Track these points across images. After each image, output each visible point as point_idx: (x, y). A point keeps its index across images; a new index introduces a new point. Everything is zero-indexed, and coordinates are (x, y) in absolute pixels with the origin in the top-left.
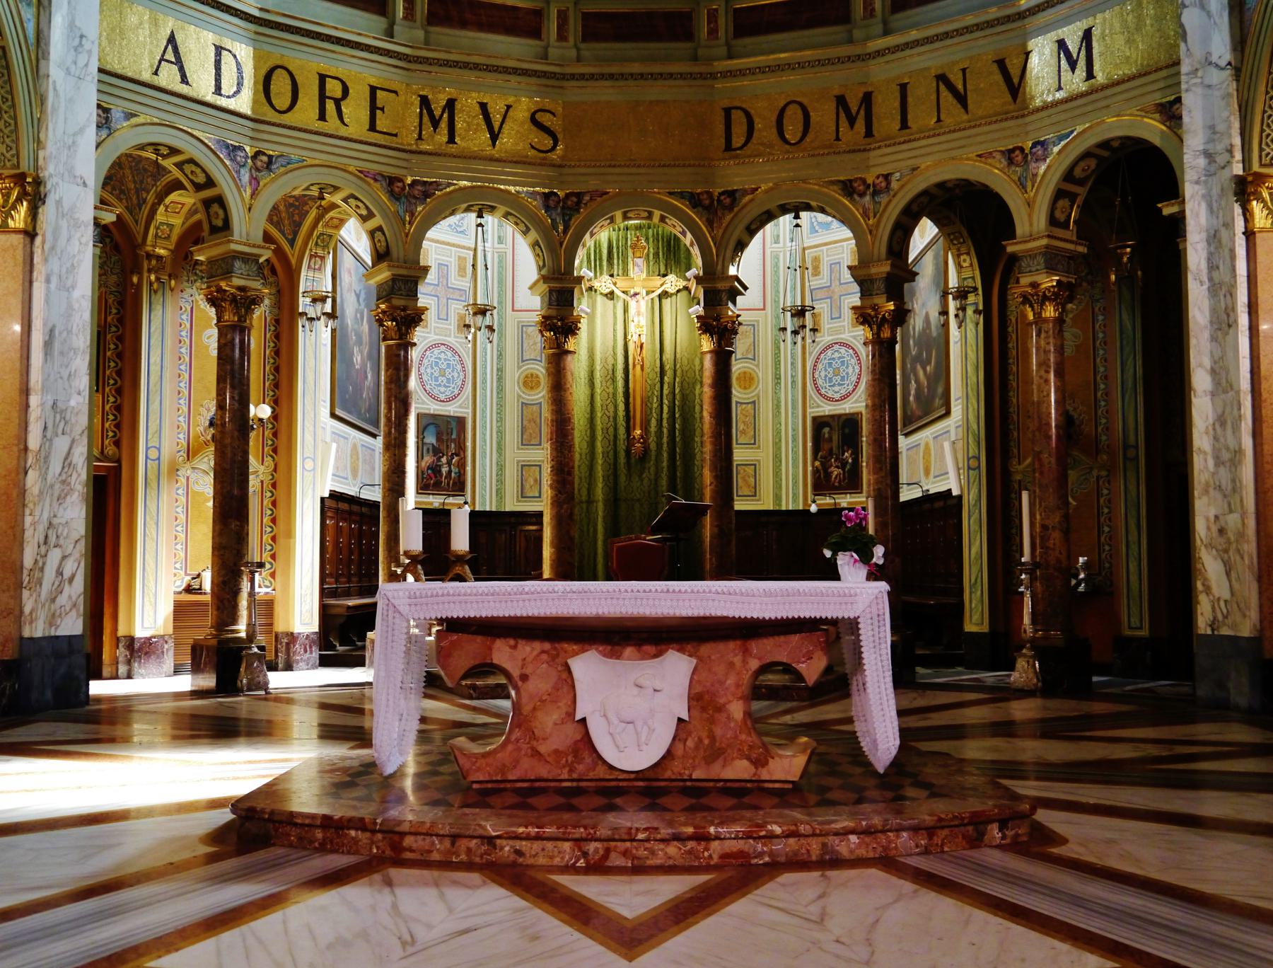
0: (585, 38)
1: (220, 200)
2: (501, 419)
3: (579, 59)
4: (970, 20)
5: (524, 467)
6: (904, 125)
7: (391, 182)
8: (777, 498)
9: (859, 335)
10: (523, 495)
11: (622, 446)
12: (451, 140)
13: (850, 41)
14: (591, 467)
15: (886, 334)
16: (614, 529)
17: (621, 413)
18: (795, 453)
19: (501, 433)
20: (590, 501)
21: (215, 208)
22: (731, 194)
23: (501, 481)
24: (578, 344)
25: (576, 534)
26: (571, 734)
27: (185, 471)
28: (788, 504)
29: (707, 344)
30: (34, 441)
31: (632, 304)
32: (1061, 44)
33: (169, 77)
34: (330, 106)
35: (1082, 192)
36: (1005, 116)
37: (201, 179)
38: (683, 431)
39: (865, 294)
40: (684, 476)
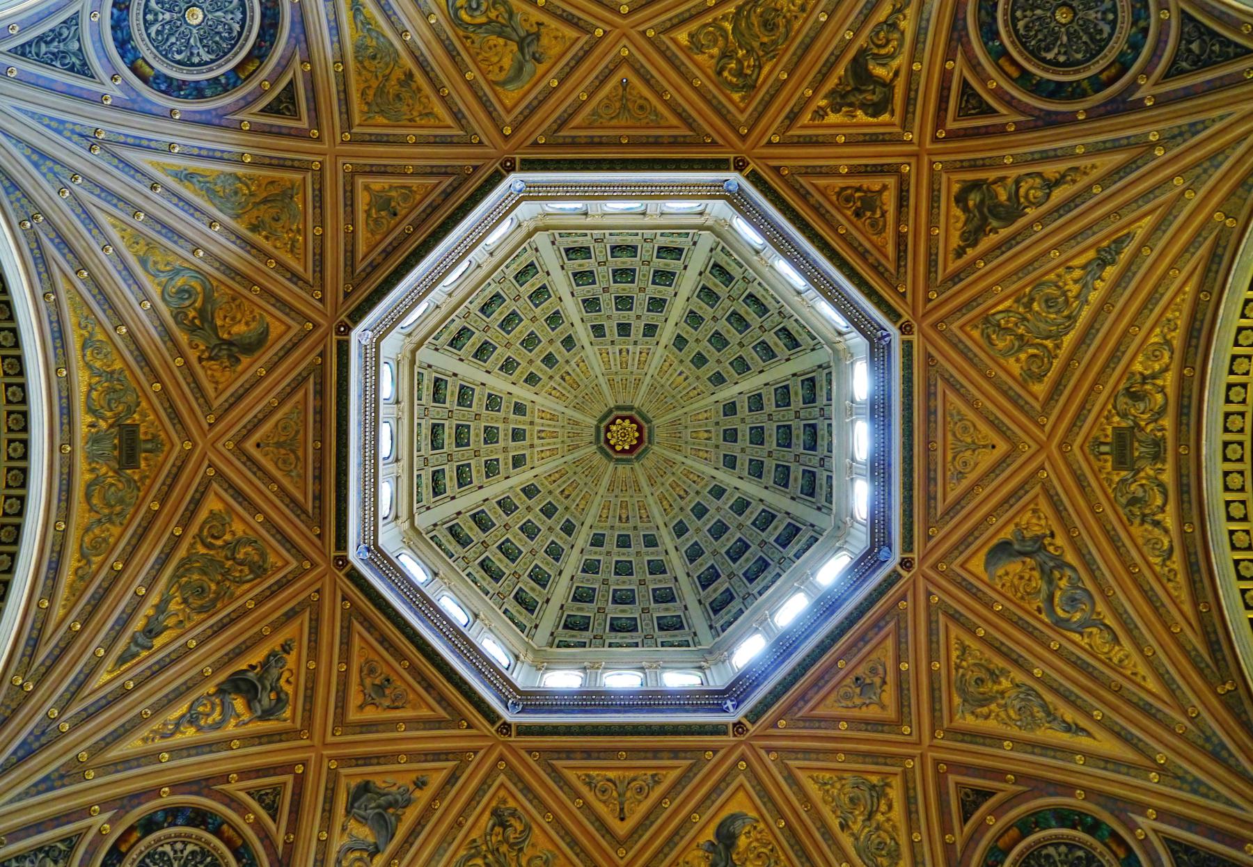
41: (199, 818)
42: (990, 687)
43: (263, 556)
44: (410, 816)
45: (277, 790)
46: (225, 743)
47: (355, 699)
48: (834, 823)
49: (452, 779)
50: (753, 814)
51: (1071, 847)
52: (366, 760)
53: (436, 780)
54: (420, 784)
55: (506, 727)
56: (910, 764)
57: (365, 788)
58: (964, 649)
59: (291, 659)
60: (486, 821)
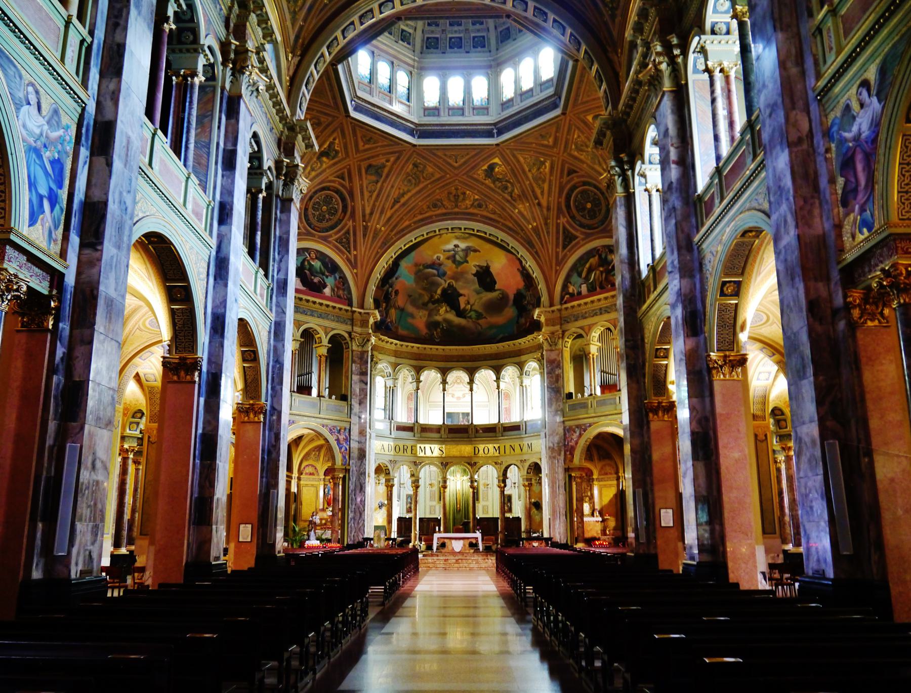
5: (431, 507)
9: (498, 489)
10: (431, 513)
16: (454, 525)
19: (425, 498)
23: (425, 509)
24: (447, 490)
29: (471, 490)
33: (382, 452)
36: (520, 454)
40: (467, 517)
41: (323, 189)
42: (584, 148)
43: (319, 120)
44: (386, 170)
45: (343, 174)
46: (324, 170)
47: (361, 144)
48: (527, 169)
49: (398, 158)
50: (500, 163)
51: (595, 194)
52: (368, 158)
53: (392, 159)
54: (388, 161)
55: (415, 146)
56: (554, 158)
57: (370, 166)
58: (579, 137)
59: (337, 141)
60: (411, 166)
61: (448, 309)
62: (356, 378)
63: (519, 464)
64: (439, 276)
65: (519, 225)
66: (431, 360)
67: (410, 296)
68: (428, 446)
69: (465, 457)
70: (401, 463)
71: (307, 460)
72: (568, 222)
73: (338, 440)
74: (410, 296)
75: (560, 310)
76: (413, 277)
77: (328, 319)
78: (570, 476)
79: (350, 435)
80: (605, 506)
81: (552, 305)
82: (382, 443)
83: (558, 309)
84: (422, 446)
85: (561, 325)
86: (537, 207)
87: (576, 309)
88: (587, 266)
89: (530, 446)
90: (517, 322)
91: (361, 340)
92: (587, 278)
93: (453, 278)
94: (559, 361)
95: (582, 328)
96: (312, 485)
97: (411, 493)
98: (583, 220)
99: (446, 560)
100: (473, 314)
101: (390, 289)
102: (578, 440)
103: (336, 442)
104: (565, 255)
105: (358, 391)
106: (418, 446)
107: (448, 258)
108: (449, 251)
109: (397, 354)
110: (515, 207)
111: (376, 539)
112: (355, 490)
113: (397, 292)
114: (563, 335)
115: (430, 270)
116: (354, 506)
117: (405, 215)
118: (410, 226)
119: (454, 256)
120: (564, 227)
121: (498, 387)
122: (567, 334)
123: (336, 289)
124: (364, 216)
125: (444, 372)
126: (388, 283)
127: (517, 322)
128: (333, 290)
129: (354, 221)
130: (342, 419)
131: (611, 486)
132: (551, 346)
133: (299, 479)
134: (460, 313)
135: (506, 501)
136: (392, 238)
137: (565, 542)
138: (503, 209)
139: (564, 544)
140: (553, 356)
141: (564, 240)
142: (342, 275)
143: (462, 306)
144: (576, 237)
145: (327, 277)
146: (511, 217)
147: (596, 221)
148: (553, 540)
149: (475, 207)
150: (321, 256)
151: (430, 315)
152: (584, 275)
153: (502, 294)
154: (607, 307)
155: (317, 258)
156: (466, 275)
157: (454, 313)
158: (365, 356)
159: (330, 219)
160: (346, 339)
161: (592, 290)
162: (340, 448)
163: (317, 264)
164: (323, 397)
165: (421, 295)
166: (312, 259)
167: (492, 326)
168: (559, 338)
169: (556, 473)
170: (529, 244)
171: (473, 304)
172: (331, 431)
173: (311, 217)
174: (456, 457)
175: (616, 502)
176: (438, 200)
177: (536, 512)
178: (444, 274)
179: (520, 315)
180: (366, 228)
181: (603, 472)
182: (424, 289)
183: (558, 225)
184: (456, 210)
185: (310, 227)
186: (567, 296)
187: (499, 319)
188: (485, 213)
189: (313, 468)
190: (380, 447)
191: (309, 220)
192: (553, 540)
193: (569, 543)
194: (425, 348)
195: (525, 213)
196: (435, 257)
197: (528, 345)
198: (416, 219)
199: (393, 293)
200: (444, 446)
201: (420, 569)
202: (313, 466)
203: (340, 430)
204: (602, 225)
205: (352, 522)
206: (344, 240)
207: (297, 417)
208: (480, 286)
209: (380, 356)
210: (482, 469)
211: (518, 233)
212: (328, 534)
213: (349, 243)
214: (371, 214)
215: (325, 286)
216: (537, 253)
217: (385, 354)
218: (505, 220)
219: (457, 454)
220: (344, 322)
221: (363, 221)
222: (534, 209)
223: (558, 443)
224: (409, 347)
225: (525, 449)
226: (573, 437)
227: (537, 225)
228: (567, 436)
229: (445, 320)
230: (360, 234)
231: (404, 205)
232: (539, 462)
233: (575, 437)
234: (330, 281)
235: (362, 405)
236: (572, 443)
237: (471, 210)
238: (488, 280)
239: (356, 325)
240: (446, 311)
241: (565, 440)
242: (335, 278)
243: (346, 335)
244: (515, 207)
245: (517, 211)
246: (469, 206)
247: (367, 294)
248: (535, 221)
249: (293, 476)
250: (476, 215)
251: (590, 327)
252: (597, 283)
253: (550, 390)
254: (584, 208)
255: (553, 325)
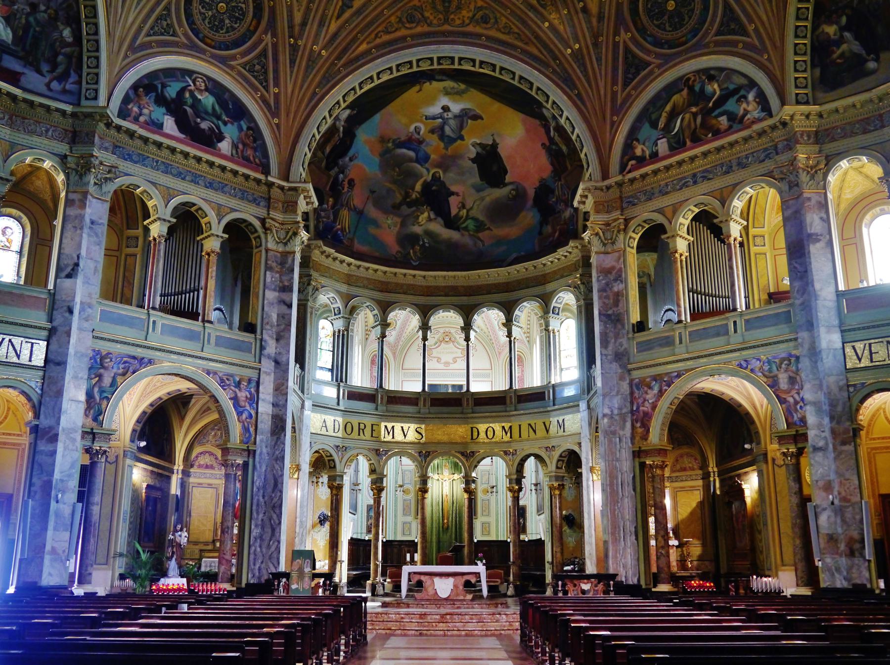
0: (431, 406)
1: (333, 460)
2: (396, 506)
3: (429, 413)
4: (536, 410)
6: (520, 436)
7: (377, 450)
8: (497, 535)
9: (510, 494)
10: (404, 534)
11: (441, 525)
12: (393, 438)
13: (506, 411)
14: (432, 532)
15: (516, 495)
16: (439, 551)
17: (441, 515)
18: (503, 519)
19: (396, 511)
20: (431, 542)
21: (331, 462)
22: (473, 452)
23: (396, 529)
24: (428, 496)
25: (427, 552)
26: (434, 591)
27: (312, 532)
28: (501, 538)
29: (466, 496)
30: (297, 530)
31: (444, 483)
32: (558, 421)
33: (324, 432)
34: (361, 431)
35: (566, 459)
36: (545, 438)
37: (329, 455)
38: (459, 521)
39: (510, 483)
40: (459, 537)
61: (432, 216)
62: (271, 295)
63: (543, 454)
64: (417, 161)
65: (550, 51)
66: (405, 293)
67: (373, 192)
68: (398, 426)
69: (456, 443)
70: (355, 452)
71: (202, 444)
72: (633, 39)
73: (235, 399)
74: (373, 192)
75: (620, 185)
76: (377, 160)
77: (224, 192)
78: (643, 465)
79: (258, 391)
80: (683, 521)
81: (605, 176)
82: (324, 417)
83: (616, 183)
84: (389, 425)
85: (622, 210)
86: (581, 15)
87: (648, 180)
88: (668, 108)
89: (562, 425)
90: (540, 233)
91: (282, 234)
92: (668, 128)
93: (439, 165)
94: (621, 268)
95: (660, 211)
96: (210, 486)
97: (372, 502)
98: (660, 34)
99: (422, 616)
100: (470, 224)
101: (341, 176)
102: (658, 400)
103: (231, 403)
104: (629, 95)
105: (274, 317)
106: (383, 424)
107: (432, 131)
108: (434, 118)
109: (349, 280)
110: (544, 19)
111: (294, 575)
112: (264, 487)
113: (351, 183)
114: (626, 226)
115: (404, 151)
116: (261, 516)
117: (361, 32)
118: (368, 52)
119: (441, 128)
120: (627, 49)
121: (509, 335)
122: (633, 224)
123: (240, 146)
124: (291, 27)
125: (425, 312)
126: (336, 164)
127: (540, 233)
128: (235, 146)
129: (274, 35)
130: (245, 363)
131: (693, 489)
132: (604, 245)
133: (186, 473)
134: (451, 223)
135: (519, 514)
136: (339, 71)
137: (636, 581)
138: (524, 22)
139: (633, 586)
140: (609, 261)
141: (626, 72)
142: (252, 125)
143: (454, 211)
144: (648, 64)
145: (225, 123)
146: (537, 37)
147: (684, 30)
148: (618, 579)
149: (477, 23)
150: (215, 88)
151: (403, 224)
152: (661, 124)
153: (516, 190)
154: (706, 171)
155: (207, 89)
156: (460, 162)
157: (442, 222)
158: (290, 261)
159: (234, 29)
160: (256, 231)
161: (677, 146)
162: (240, 414)
163: (208, 100)
164: (210, 322)
165: (389, 191)
166: (201, 91)
167: (499, 241)
168: (619, 231)
169: (617, 460)
170: (566, 82)
171: (471, 208)
172: (222, 383)
173: (197, 18)
174: (444, 443)
175: (703, 513)
176: (415, 8)
177: (568, 531)
178: (427, 158)
179: (543, 222)
180: (294, 48)
181: (678, 467)
182: (395, 182)
183: (616, 45)
184: (446, 27)
185: (197, 36)
186: (633, 162)
187: (511, 231)
188: (493, 33)
189: (213, 458)
190: (319, 424)
191: (193, 23)
192: (618, 579)
193: (643, 583)
194: (395, 274)
195: (561, 28)
196: (412, 128)
197: (557, 265)
198: (378, 41)
199: (346, 186)
200: (423, 426)
201: (369, 637)
202: (211, 454)
203: (239, 383)
204: (695, 36)
205: (258, 544)
206: (258, 67)
207: (158, 353)
208: (481, 179)
209: (323, 280)
210: (482, 463)
211: (547, 65)
212: (209, 564)
213: (266, 73)
214: (304, 24)
215: (221, 138)
216: (579, 95)
217: (330, 277)
218: (526, 44)
219: (445, 438)
220: (255, 201)
221: (290, 37)
222: (575, 18)
223: (620, 409)
224: (370, 271)
225: (553, 429)
226: (648, 397)
227: (580, 47)
228: (636, 395)
229: (428, 233)
230: (284, 58)
231: (359, 12)
232: (576, 449)
233: (651, 396)
234: (230, 132)
235: (282, 342)
236: (647, 407)
237: (470, 29)
238: (495, 168)
239: (275, 209)
240: (430, 219)
241: (632, 403)
242: (240, 129)
243: (257, 224)
244: (544, 19)
245: (547, 24)
246: (467, 21)
247: (295, 159)
248: (577, 41)
249: (176, 468)
250: (479, 36)
251: (676, 209)
252: (687, 133)
253: (604, 318)
254: (663, 12)
255: (608, 212)
